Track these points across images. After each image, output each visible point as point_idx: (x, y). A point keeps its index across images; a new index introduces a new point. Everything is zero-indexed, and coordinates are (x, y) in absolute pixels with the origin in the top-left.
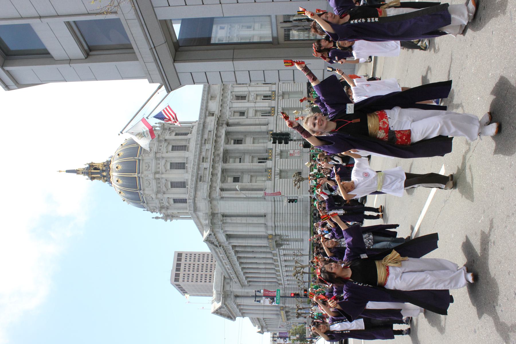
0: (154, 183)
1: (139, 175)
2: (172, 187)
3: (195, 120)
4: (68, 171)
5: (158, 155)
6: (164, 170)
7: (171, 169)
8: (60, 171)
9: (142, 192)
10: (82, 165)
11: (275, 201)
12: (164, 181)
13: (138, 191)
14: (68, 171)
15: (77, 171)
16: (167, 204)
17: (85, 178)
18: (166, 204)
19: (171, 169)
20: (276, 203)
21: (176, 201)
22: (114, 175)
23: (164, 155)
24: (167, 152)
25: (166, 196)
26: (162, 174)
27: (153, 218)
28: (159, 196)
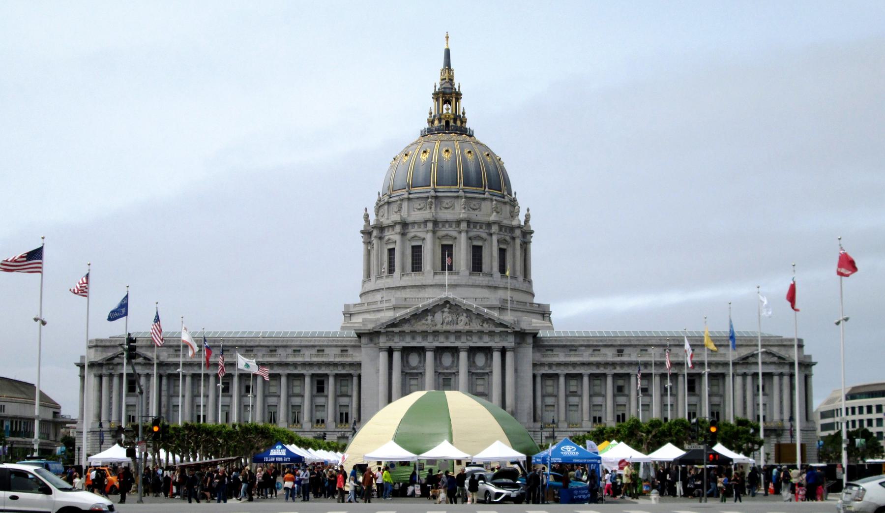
1: (461, 193)
3: (542, 290)
4: (448, 52)
5: (495, 229)
6: (472, 234)
8: (447, 38)
10: (459, 81)
12: (454, 234)
14: (448, 52)
17: (435, 81)
18: (412, 232)
21: (417, 251)
23: (495, 238)
24: (498, 241)
25: (429, 237)
28: (430, 226)
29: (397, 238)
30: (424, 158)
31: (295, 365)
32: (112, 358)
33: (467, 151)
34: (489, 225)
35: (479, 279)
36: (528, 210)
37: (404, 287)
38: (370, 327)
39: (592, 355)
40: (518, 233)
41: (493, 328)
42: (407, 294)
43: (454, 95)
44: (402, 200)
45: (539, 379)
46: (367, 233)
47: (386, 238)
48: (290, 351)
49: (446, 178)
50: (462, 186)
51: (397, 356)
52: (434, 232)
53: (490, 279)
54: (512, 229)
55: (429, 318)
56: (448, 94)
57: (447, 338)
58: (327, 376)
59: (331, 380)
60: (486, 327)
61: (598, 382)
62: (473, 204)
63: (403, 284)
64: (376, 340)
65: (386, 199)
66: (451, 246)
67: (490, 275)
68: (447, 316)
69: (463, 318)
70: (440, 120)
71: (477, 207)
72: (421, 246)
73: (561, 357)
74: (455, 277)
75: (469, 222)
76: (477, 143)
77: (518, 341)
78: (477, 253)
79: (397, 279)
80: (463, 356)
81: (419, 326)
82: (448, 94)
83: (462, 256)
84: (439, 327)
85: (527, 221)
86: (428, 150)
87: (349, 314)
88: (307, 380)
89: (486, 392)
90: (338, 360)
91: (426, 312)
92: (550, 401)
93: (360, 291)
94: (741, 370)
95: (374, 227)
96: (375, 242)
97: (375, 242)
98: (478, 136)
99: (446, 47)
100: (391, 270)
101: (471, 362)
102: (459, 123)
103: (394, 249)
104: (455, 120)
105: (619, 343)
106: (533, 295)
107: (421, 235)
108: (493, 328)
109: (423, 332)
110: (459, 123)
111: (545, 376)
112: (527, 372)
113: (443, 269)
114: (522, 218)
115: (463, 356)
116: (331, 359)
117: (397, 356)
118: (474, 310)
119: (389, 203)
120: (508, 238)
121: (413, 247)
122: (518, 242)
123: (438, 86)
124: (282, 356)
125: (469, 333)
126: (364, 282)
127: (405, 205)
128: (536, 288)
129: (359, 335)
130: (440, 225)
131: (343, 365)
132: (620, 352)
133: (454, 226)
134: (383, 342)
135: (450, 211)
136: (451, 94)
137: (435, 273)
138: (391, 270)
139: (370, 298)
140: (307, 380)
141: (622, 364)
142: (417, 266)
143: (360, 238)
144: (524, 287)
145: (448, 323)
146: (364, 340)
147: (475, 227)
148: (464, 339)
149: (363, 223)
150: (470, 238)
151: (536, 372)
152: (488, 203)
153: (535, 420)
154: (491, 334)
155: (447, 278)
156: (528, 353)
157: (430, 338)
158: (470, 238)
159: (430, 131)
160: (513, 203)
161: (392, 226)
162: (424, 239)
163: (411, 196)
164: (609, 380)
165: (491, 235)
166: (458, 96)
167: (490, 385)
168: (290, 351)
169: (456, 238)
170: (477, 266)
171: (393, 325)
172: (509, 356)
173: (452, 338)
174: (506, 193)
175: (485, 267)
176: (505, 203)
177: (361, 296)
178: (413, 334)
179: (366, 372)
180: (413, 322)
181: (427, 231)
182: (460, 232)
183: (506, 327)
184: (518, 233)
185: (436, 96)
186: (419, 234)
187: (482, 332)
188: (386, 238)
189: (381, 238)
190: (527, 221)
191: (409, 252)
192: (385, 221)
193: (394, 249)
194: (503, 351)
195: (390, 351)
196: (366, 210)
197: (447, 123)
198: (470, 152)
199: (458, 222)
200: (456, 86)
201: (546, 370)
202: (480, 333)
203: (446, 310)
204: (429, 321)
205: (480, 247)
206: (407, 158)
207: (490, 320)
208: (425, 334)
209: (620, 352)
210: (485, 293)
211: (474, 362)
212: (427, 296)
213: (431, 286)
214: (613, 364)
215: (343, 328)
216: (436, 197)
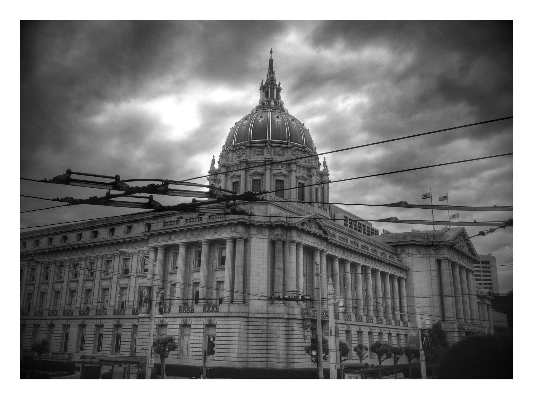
0: (260, 158)
2: (253, 180)
4: (271, 61)
7: (276, 180)
8: (271, 52)
11: (268, 318)
13: (249, 140)
14: (271, 61)
15: (273, 72)
19: (276, 180)
20: (266, 320)
22: (268, 115)
23: (293, 173)
24: (297, 177)
25: (243, 173)
26: (271, 170)
27: (214, 157)
28: (244, 166)
33: (275, 117)
66: (260, 180)
71: (281, 153)
75: (272, 163)
120: (305, 176)
158: (274, 175)
163: (234, 149)
165: (290, 172)
169: (262, 175)
182: (265, 170)
198: (278, 117)
200: (277, 83)
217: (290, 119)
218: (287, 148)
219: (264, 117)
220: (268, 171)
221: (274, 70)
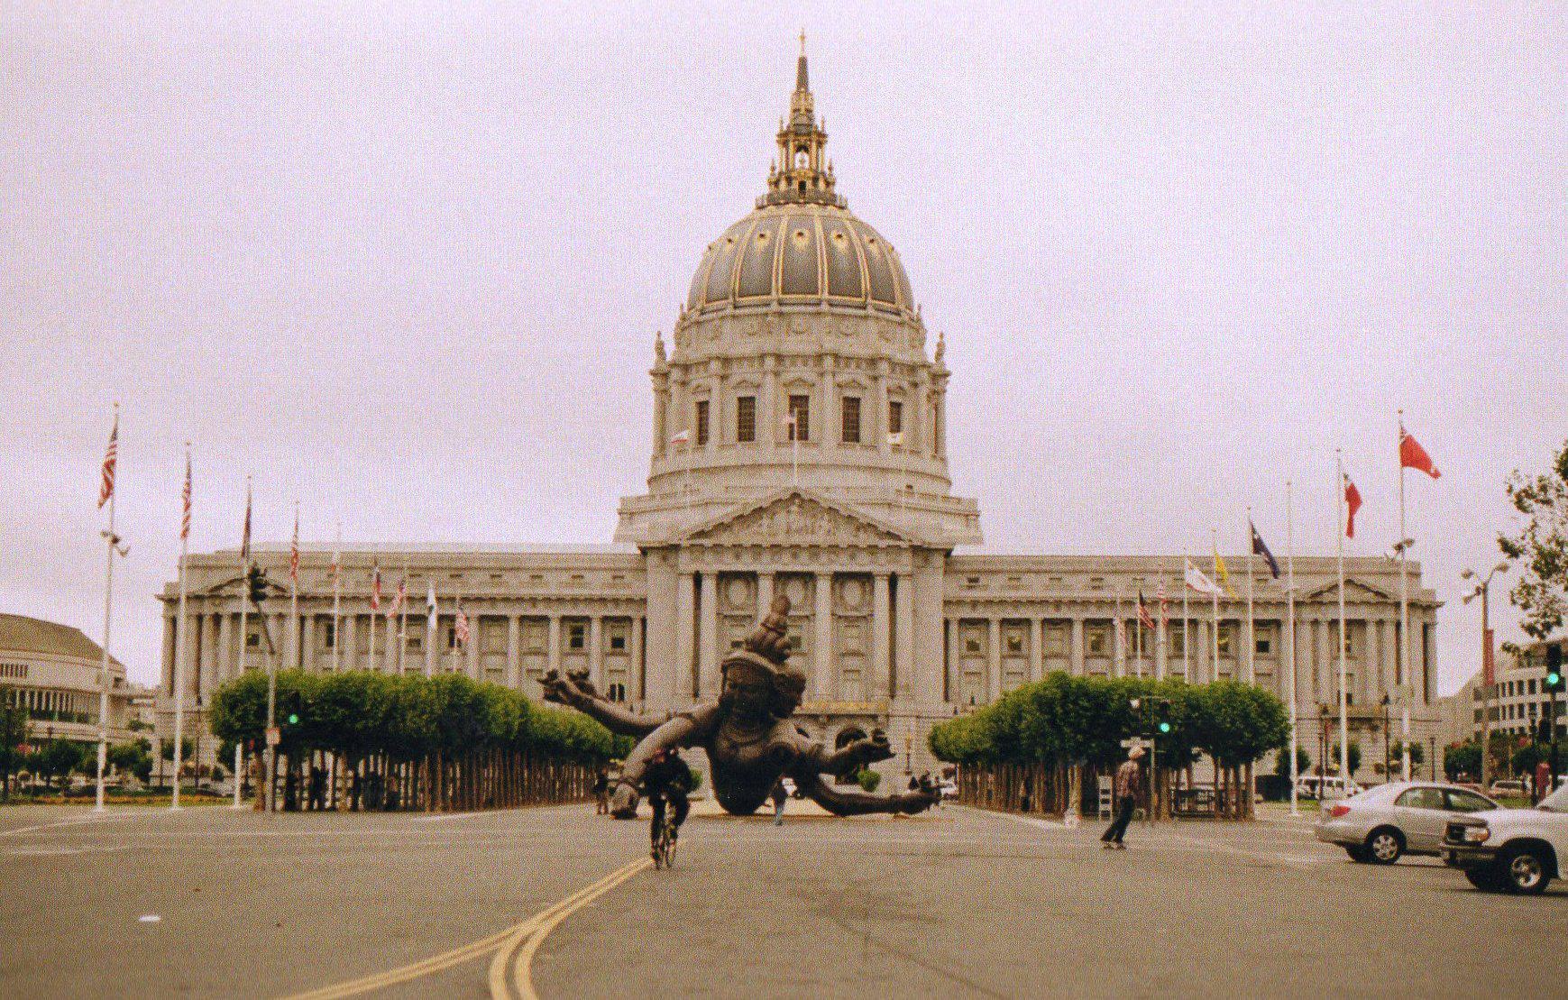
0: (811, 349)
1: (825, 307)
3: (967, 473)
4: (803, 63)
6: (842, 378)
9: (775, 307)
10: (823, 115)
14: (803, 63)
16: (735, 379)
17: (782, 115)
21: (746, 405)
23: (883, 385)
24: (889, 391)
29: (715, 383)
30: (761, 244)
31: (533, 601)
32: (219, 587)
33: (834, 234)
34: (873, 362)
35: (855, 454)
36: (942, 336)
37: (725, 469)
38: (662, 537)
39: (1047, 588)
40: (923, 375)
41: (873, 540)
42: (734, 480)
43: (814, 137)
44: (723, 318)
45: (954, 628)
46: (661, 375)
47: (694, 383)
48: (525, 576)
49: (799, 283)
50: (826, 296)
51: (709, 586)
52: (777, 374)
53: (875, 453)
54: (913, 369)
55: (766, 521)
56: (802, 134)
57: (795, 556)
58: (588, 619)
59: (596, 627)
60: (865, 539)
61: (1056, 634)
62: (847, 326)
63: (723, 463)
64: (672, 560)
65: (695, 316)
66: (807, 398)
67: (873, 447)
68: (795, 517)
69: (825, 524)
70: (789, 180)
72: (752, 399)
73: (994, 588)
74: (814, 451)
75: (836, 357)
76: (853, 220)
77: (919, 561)
78: (852, 405)
79: (713, 454)
80: (824, 586)
81: (746, 537)
82: (802, 134)
83: (826, 415)
84: (781, 539)
85: (939, 355)
86: (768, 233)
87: (629, 513)
88: (554, 626)
89: (863, 649)
90: (606, 593)
91: (759, 511)
92: (974, 665)
93: (646, 475)
94: (1308, 614)
95: (674, 365)
96: (674, 389)
97: (674, 389)
98: (856, 209)
99: (799, 54)
100: (702, 438)
101: (838, 599)
102: (821, 185)
103: (707, 403)
104: (815, 180)
105: (1094, 567)
106: (949, 483)
107: (756, 378)
108: (873, 540)
109: (754, 546)
110: (821, 185)
111: (964, 622)
112: (936, 616)
113: (791, 438)
114: (930, 351)
115: (824, 586)
116: (597, 593)
117: (709, 586)
118: (842, 512)
119: (698, 323)
120: (905, 385)
121: (740, 399)
122: (924, 390)
123: (787, 122)
124: (515, 585)
125: (834, 549)
126: (655, 458)
127: (728, 327)
128: (953, 472)
129: (644, 551)
130: (787, 362)
131: (616, 601)
132: (1097, 583)
133: (811, 363)
134: (686, 563)
135: (804, 337)
136: (809, 134)
137: (778, 444)
138: (702, 438)
139: (666, 487)
140: (554, 626)
141: (1100, 603)
142: (746, 432)
143: (648, 385)
144: (933, 467)
145: (799, 531)
146: (653, 559)
147: (847, 366)
148: (824, 558)
149: (655, 357)
150: (839, 386)
151: (949, 616)
152: (872, 324)
153: (947, 698)
154: (872, 549)
155: (797, 452)
156: (936, 585)
157: (766, 557)
158: (839, 386)
159: (773, 201)
160: (916, 326)
161: (705, 363)
162: (758, 386)
164: (1078, 629)
165: (875, 379)
166: (821, 138)
167: (869, 639)
168: (525, 576)
170: (851, 432)
171: (701, 534)
172: (903, 585)
173: (804, 556)
174: (902, 307)
175: (865, 433)
176: (901, 324)
177: (650, 482)
178: (737, 549)
179: (654, 613)
180: (736, 528)
181: (765, 373)
182: (822, 375)
183: (898, 538)
184: (923, 375)
185: (784, 139)
186: (748, 377)
187: (856, 546)
188: (694, 383)
189: (684, 384)
190: (939, 355)
191: (733, 409)
192: (693, 355)
193: (707, 403)
194: (893, 580)
195: (698, 579)
196: (659, 334)
197: (802, 185)
199: (819, 357)
201: (967, 613)
202: (854, 549)
203: (794, 508)
204: (764, 529)
205: (858, 400)
206: (729, 247)
207: (870, 527)
208: (757, 549)
209: (1097, 583)
210: (861, 479)
211: (842, 597)
212: (761, 482)
213: (772, 466)
214: (1085, 603)
215: (617, 538)
216: (781, 314)
217: (866, 239)
218: (866, 317)
219: (806, 232)
220: (829, 378)
221: (811, 88)
